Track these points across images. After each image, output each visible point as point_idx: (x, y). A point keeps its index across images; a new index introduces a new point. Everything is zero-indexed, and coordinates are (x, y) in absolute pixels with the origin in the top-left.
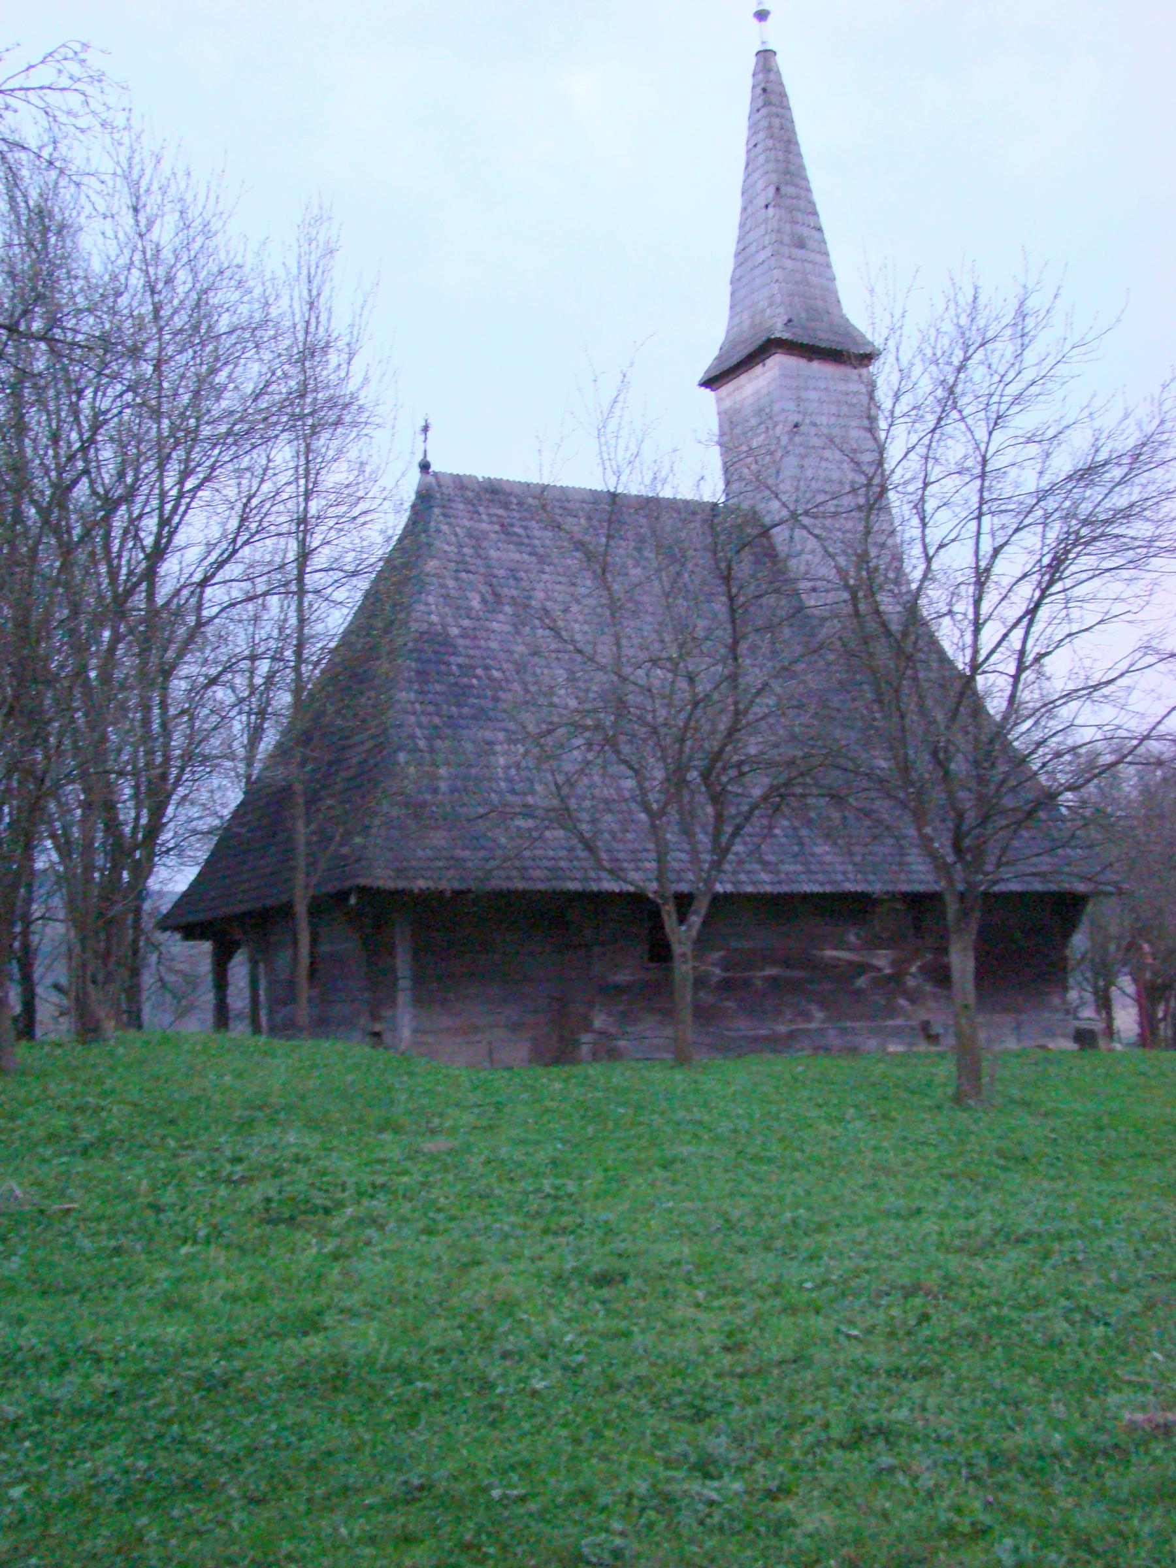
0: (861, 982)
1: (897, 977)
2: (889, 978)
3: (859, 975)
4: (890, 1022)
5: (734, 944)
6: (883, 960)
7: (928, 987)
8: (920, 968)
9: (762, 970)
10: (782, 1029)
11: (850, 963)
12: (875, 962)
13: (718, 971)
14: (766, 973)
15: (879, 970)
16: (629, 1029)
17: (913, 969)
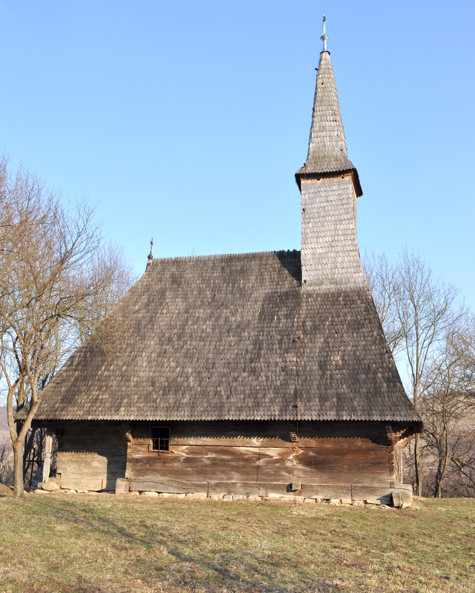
0: (261, 462)
1: (282, 460)
2: (277, 461)
3: (259, 459)
4: (276, 483)
5: (191, 443)
6: (274, 452)
7: (300, 467)
8: (297, 457)
9: (207, 454)
10: (213, 482)
11: (255, 453)
12: (268, 453)
13: (184, 454)
14: (209, 456)
15: (271, 457)
16: (142, 478)
17: (291, 457)
